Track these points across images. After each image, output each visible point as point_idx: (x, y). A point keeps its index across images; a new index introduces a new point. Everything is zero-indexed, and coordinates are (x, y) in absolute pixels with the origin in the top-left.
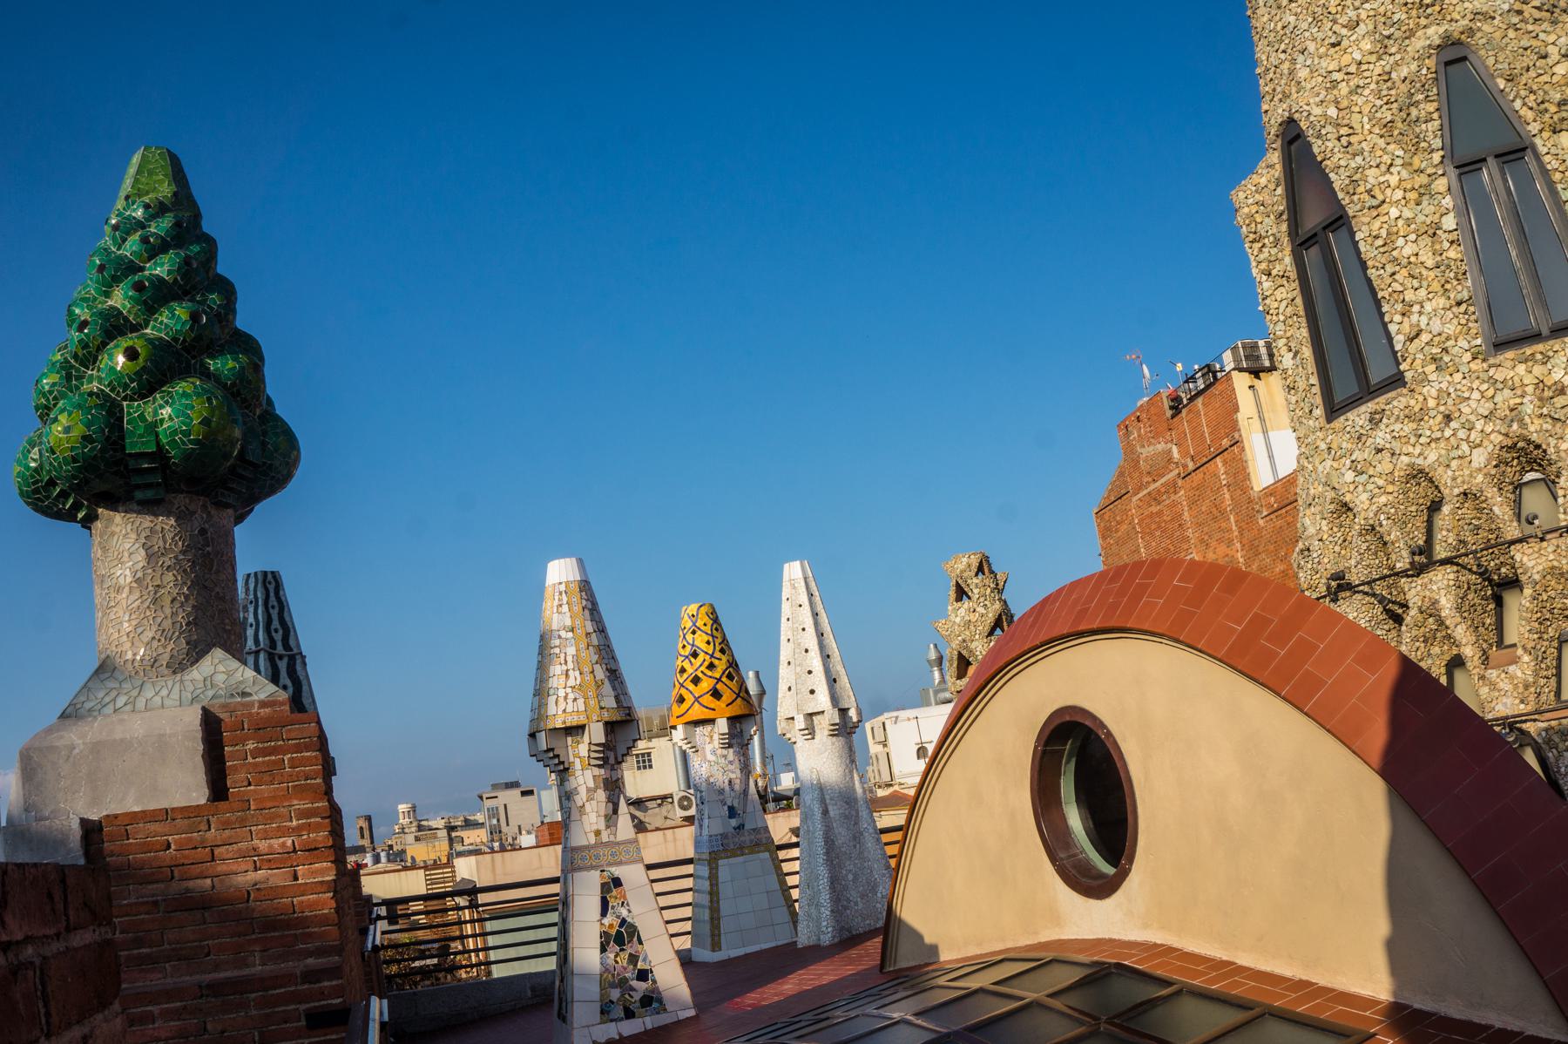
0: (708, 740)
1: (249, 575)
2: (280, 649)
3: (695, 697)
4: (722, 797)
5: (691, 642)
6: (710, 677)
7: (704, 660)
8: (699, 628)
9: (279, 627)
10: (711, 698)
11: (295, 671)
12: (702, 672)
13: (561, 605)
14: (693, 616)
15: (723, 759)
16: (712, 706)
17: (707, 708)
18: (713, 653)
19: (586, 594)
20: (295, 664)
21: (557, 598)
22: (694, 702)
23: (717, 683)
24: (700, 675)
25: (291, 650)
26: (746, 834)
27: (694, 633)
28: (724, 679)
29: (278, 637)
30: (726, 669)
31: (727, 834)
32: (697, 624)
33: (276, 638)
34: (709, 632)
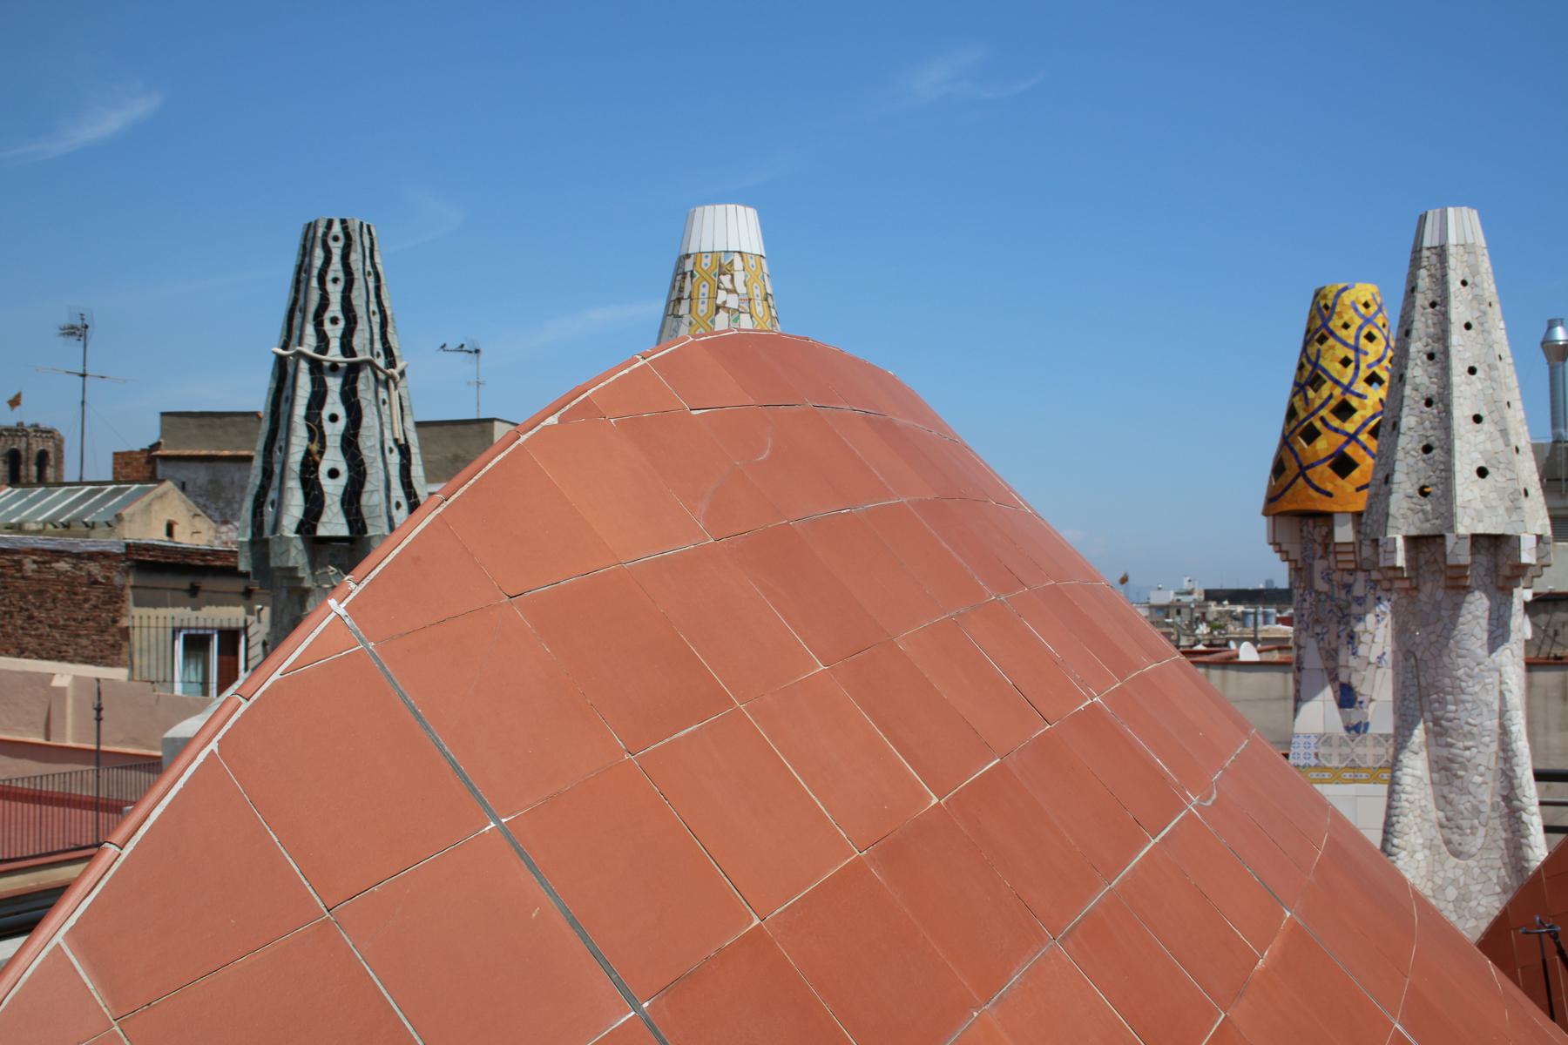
0: (1319, 550)
1: (310, 224)
2: (334, 354)
3: (1300, 466)
4: (1331, 664)
5: (1313, 358)
6: (1336, 430)
7: (1331, 397)
8: (1332, 333)
9: (340, 315)
10: (1329, 472)
11: (354, 391)
12: (1323, 419)
13: (679, 300)
14: (1326, 307)
15: (1343, 594)
16: (1329, 487)
17: (1317, 489)
18: (1351, 383)
19: (732, 280)
20: (355, 380)
21: (677, 284)
22: (1297, 477)
23: (1347, 443)
24: (1318, 425)
25: (354, 354)
26: (1370, 742)
27: (1322, 340)
28: (1363, 437)
29: (334, 332)
30: (1373, 417)
31: (1330, 738)
32: (1331, 325)
33: (330, 334)
34: (1351, 342)
